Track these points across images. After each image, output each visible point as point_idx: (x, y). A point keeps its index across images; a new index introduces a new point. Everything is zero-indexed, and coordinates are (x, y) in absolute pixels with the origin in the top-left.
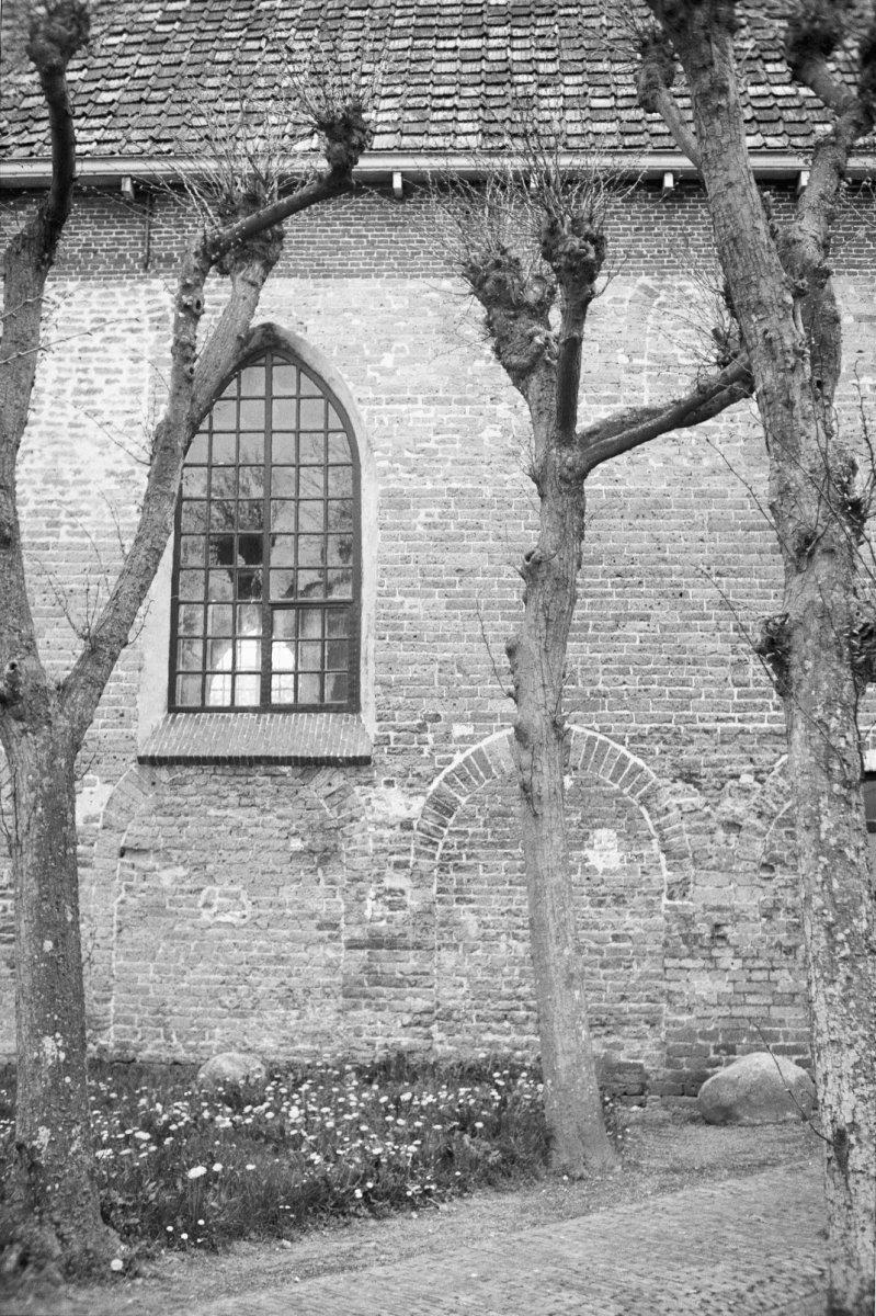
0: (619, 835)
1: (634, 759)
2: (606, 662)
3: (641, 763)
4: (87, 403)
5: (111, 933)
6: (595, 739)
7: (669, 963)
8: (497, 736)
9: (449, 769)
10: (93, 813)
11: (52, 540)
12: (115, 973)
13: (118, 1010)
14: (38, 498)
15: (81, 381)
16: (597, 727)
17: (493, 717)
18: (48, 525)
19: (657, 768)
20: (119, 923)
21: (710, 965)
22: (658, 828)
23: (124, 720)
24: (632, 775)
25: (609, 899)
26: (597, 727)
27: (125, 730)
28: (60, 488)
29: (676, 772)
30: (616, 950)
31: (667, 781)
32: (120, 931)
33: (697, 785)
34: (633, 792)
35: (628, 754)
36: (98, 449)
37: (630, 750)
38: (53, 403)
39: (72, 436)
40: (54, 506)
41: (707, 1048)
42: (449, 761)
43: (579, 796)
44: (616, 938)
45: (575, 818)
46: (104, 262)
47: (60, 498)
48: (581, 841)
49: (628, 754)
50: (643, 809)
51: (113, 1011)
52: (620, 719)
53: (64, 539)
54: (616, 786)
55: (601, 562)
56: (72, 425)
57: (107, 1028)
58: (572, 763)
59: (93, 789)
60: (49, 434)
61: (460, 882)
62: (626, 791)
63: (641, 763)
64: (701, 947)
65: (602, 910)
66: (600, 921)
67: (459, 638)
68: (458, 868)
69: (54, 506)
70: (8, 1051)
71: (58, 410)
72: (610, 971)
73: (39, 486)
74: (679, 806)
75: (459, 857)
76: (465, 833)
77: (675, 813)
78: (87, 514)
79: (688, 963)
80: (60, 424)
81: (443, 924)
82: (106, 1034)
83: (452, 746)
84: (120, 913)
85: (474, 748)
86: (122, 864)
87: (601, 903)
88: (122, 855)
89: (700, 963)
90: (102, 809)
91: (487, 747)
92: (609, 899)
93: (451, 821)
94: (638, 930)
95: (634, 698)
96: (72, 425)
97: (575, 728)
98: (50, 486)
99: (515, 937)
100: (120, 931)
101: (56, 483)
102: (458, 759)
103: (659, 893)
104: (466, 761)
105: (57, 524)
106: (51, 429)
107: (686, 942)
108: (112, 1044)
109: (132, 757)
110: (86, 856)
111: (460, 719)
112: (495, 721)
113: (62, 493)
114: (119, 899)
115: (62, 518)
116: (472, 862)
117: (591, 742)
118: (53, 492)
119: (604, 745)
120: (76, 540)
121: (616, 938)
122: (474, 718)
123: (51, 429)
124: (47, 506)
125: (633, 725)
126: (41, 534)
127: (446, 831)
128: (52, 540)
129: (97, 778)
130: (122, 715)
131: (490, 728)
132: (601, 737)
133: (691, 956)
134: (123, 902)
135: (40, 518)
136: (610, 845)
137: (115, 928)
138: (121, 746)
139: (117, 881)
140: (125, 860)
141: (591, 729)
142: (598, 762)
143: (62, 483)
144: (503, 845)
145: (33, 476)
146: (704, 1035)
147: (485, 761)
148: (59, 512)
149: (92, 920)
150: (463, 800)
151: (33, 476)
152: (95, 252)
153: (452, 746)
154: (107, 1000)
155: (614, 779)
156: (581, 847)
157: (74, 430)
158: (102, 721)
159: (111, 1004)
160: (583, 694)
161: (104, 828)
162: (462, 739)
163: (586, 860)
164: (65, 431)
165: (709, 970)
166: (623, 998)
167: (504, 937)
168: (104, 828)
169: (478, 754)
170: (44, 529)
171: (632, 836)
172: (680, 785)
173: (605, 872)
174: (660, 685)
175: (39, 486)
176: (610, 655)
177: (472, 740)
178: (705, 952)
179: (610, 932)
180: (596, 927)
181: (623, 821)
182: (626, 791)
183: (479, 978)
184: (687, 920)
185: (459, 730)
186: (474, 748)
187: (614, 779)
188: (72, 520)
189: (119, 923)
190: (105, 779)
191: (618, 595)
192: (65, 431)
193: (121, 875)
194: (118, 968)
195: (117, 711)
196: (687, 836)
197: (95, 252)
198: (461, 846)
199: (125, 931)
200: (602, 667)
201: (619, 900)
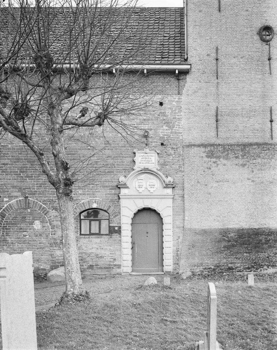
0: (40, 222)
1: (43, 205)
2: (37, 184)
3: (45, 206)
6: (35, 201)
7: (51, 248)
8: (13, 201)
9: (4, 208)
16: (35, 199)
17: (13, 197)
19: (48, 207)
21: (59, 248)
22: (49, 220)
24: (43, 209)
25: (38, 235)
26: (35, 199)
29: (53, 208)
30: (39, 246)
31: (51, 210)
33: (57, 211)
34: (43, 213)
35: (42, 204)
37: (43, 203)
41: (58, 265)
42: (4, 206)
43: (31, 214)
44: (40, 243)
45: (31, 218)
48: (32, 223)
49: (42, 204)
50: (45, 216)
52: (40, 197)
54: (40, 211)
55: (35, 162)
58: (30, 207)
61: (7, 232)
62: (42, 212)
63: (45, 206)
64: (58, 245)
65: (37, 237)
66: (37, 240)
67: (4, 179)
68: (6, 229)
72: (39, 250)
74: (53, 215)
75: (6, 226)
76: (8, 221)
77: (52, 217)
79: (55, 248)
81: (3, 241)
83: (4, 203)
85: (9, 203)
87: (37, 236)
89: (57, 248)
91: (12, 203)
92: (38, 235)
93: (5, 219)
94: (44, 241)
95: (43, 192)
97: (30, 199)
99: (19, 243)
102: (5, 206)
103: (49, 234)
104: (7, 206)
107: (54, 244)
111: (5, 197)
112: (13, 197)
116: (9, 227)
117: (34, 201)
119: (37, 203)
121: (40, 243)
122: (8, 197)
125: (43, 198)
127: (4, 221)
131: (12, 199)
132: (36, 201)
133: (56, 247)
136: (38, 224)
141: (34, 199)
142: (35, 207)
144: (16, 224)
146: (58, 263)
147: (11, 206)
150: (7, 214)
153: (4, 203)
155: (39, 210)
156: (32, 224)
160: (32, 191)
162: (6, 201)
163: (34, 227)
165: (59, 249)
166: (42, 255)
167: (16, 243)
169: (10, 204)
171: (42, 222)
172: (54, 211)
173: (37, 229)
174: (49, 189)
176: (37, 183)
177: (8, 202)
178: (58, 246)
179: (39, 242)
180: (36, 241)
181: (41, 219)
182: (42, 212)
183: (12, 252)
184: (55, 239)
185: (5, 199)
186: (9, 203)
187: (39, 210)
191: (39, 169)
196: (55, 222)
198: (7, 224)
200: (36, 186)
201: (40, 235)
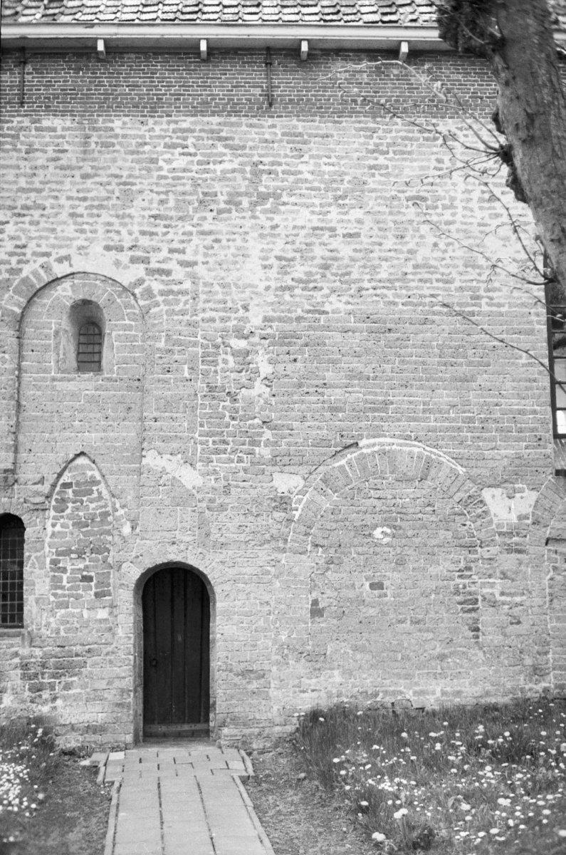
4: (489, 208)
5: (545, 603)
10: (524, 513)
11: (476, 309)
12: (551, 632)
13: (555, 660)
14: (463, 278)
15: (483, 192)
18: (472, 298)
20: (551, 594)
23: (541, 443)
27: (543, 451)
28: (478, 271)
32: (551, 601)
36: (502, 243)
38: (465, 208)
39: (481, 232)
40: (474, 283)
46: (489, 106)
47: (478, 278)
51: (551, 661)
53: (485, 308)
56: (479, 225)
57: (548, 674)
59: (523, 495)
60: (465, 231)
69: (474, 283)
70: (476, 695)
71: (469, 213)
73: (461, 269)
78: (500, 290)
80: (471, 223)
82: (547, 678)
84: (550, 587)
86: (549, 550)
88: (547, 544)
90: (531, 510)
96: (479, 225)
98: (469, 269)
100: (551, 601)
101: (474, 267)
105: (478, 298)
106: (465, 227)
108: (553, 686)
109: (550, 470)
110: (521, 545)
113: (480, 275)
114: (549, 577)
115: (482, 293)
118: (473, 274)
120: (494, 309)
123: (465, 227)
124: (469, 284)
126: (468, 305)
128: (476, 309)
129: (525, 486)
130: (540, 439)
134: (552, 579)
135: (465, 293)
137: (548, 599)
138: (541, 463)
139: (546, 563)
140: (549, 547)
143: (479, 267)
145: (456, 261)
148: (479, 289)
149: (530, 593)
151: (456, 261)
152: (481, 98)
154: (546, 653)
157: (482, 228)
158: (525, 444)
159: (550, 656)
161: (534, 523)
164: (475, 230)
168: (534, 523)
170: (469, 301)
175: (461, 269)
188: (490, 294)
189: (551, 594)
190: (531, 487)
192: (475, 230)
193: (549, 559)
194: (553, 628)
195: (536, 436)
197: (481, 98)
199: (555, 601)
